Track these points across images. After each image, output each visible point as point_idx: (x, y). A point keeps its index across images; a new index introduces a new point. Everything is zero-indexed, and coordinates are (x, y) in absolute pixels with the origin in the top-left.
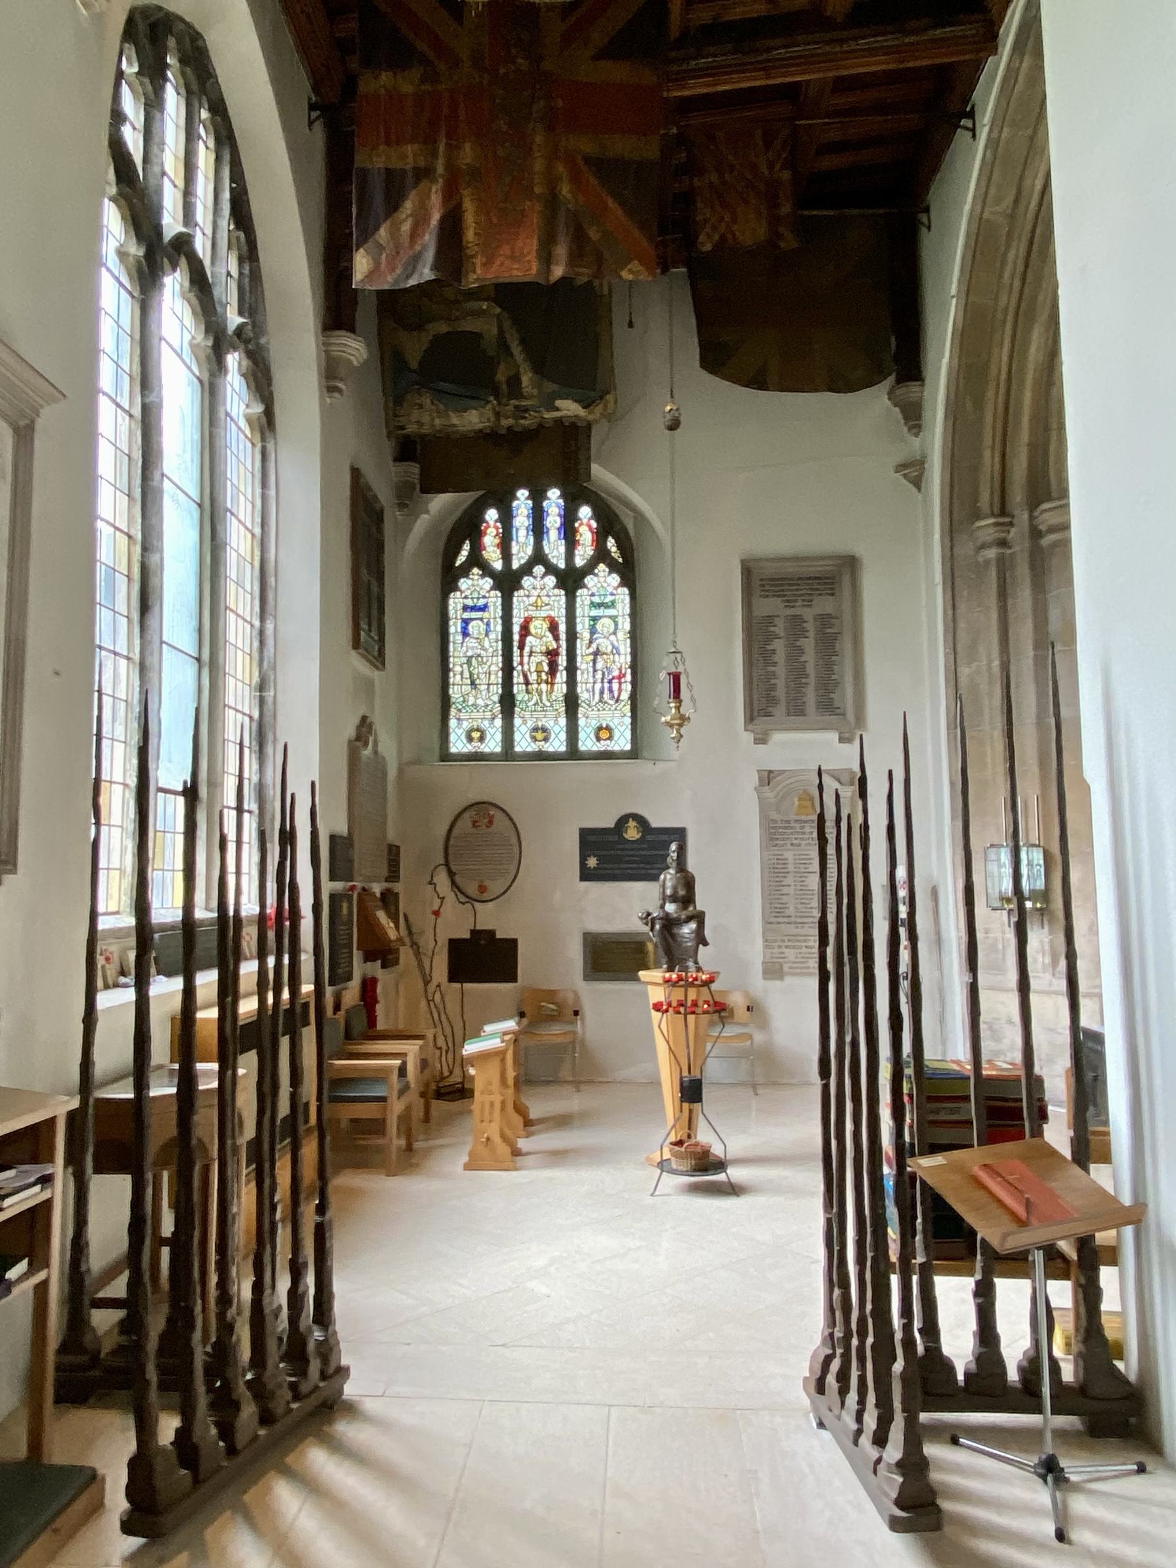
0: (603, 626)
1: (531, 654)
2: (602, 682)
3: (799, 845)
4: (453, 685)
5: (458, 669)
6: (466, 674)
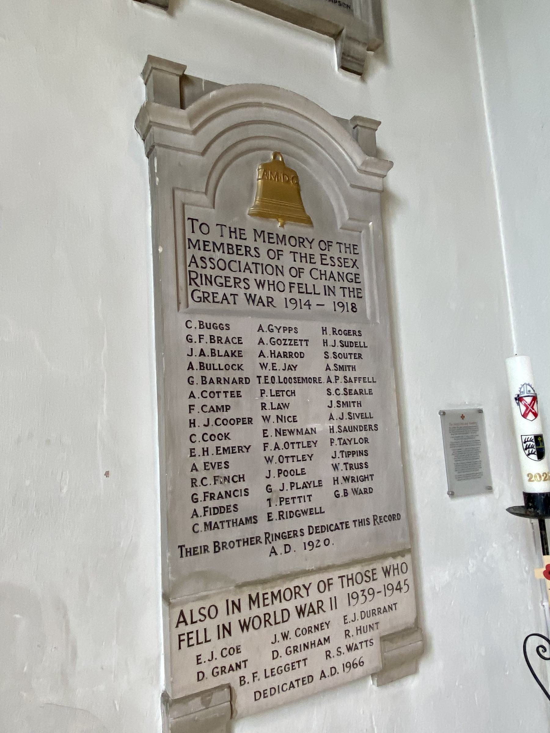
3: (270, 302)
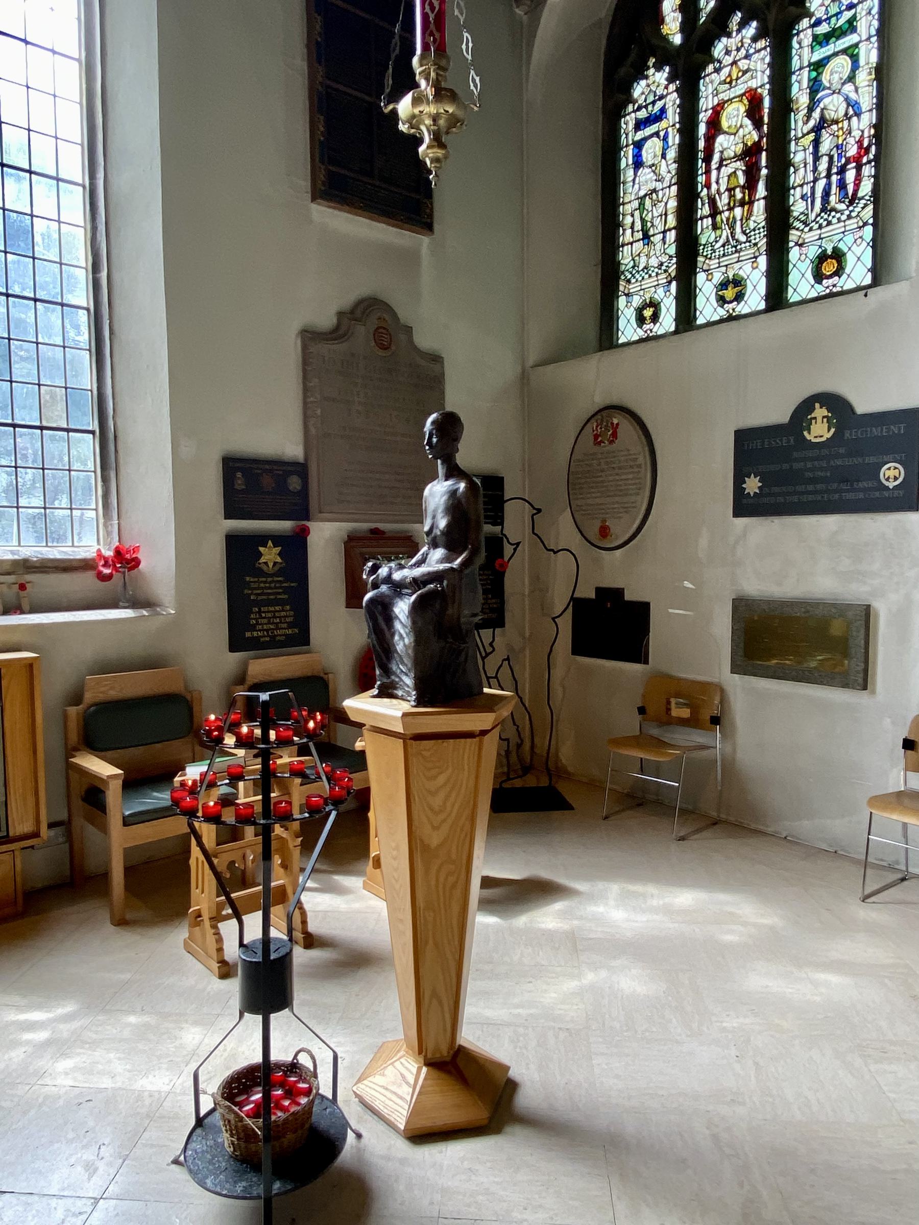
4: (623, 246)
5: (628, 220)
6: (638, 226)
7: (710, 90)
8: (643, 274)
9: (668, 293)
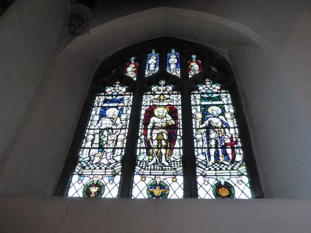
0: (212, 110)
1: (153, 128)
2: (216, 147)
4: (84, 148)
5: (91, 137)
6: (97, 141)
7: (149, 99)
8: (96, 166)
9: (111, 182)
